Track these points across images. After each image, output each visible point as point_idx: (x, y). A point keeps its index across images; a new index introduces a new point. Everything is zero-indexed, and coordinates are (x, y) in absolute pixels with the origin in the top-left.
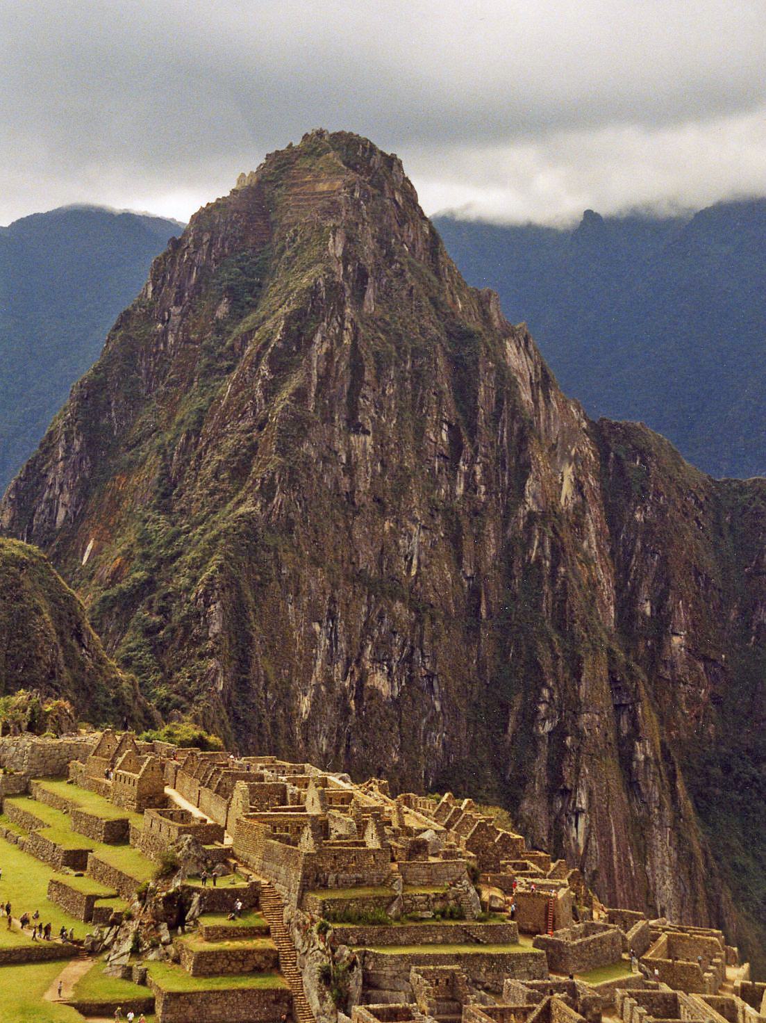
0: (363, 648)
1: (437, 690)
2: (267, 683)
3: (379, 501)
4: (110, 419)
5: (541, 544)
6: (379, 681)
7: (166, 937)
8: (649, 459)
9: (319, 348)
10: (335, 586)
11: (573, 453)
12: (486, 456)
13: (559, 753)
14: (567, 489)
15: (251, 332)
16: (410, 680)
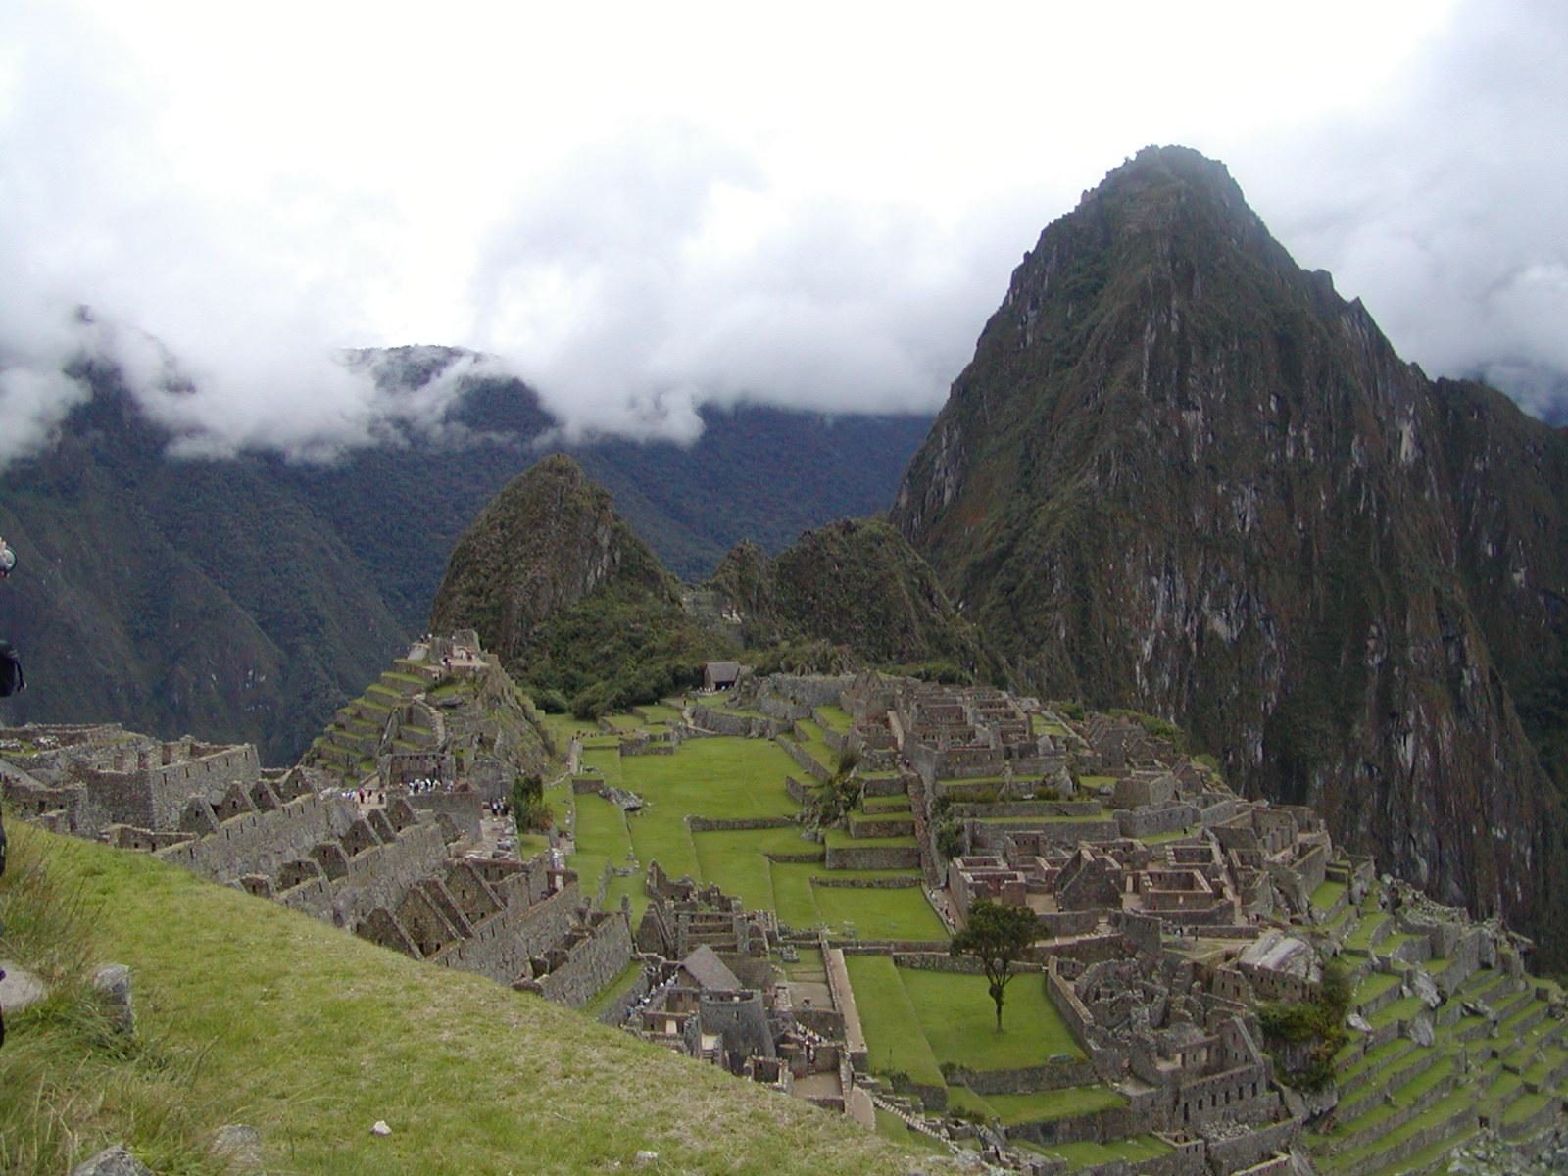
0: (1201, 597)
1: (1273, 632)
2: (1107, 630)
3: (1211, 467)
4: (983, 410)
5: (1368, 497)
6: (1219, 625)
7: (842, 813)
8: (1486, 413)
9: (1149, 338)
10: (1171, 545)
11: (1411, 411)
12: (1313, 422)
13: (1387, 681)
14: (1407, 445)
15: (1093, 328)
16: (1249, 622)
